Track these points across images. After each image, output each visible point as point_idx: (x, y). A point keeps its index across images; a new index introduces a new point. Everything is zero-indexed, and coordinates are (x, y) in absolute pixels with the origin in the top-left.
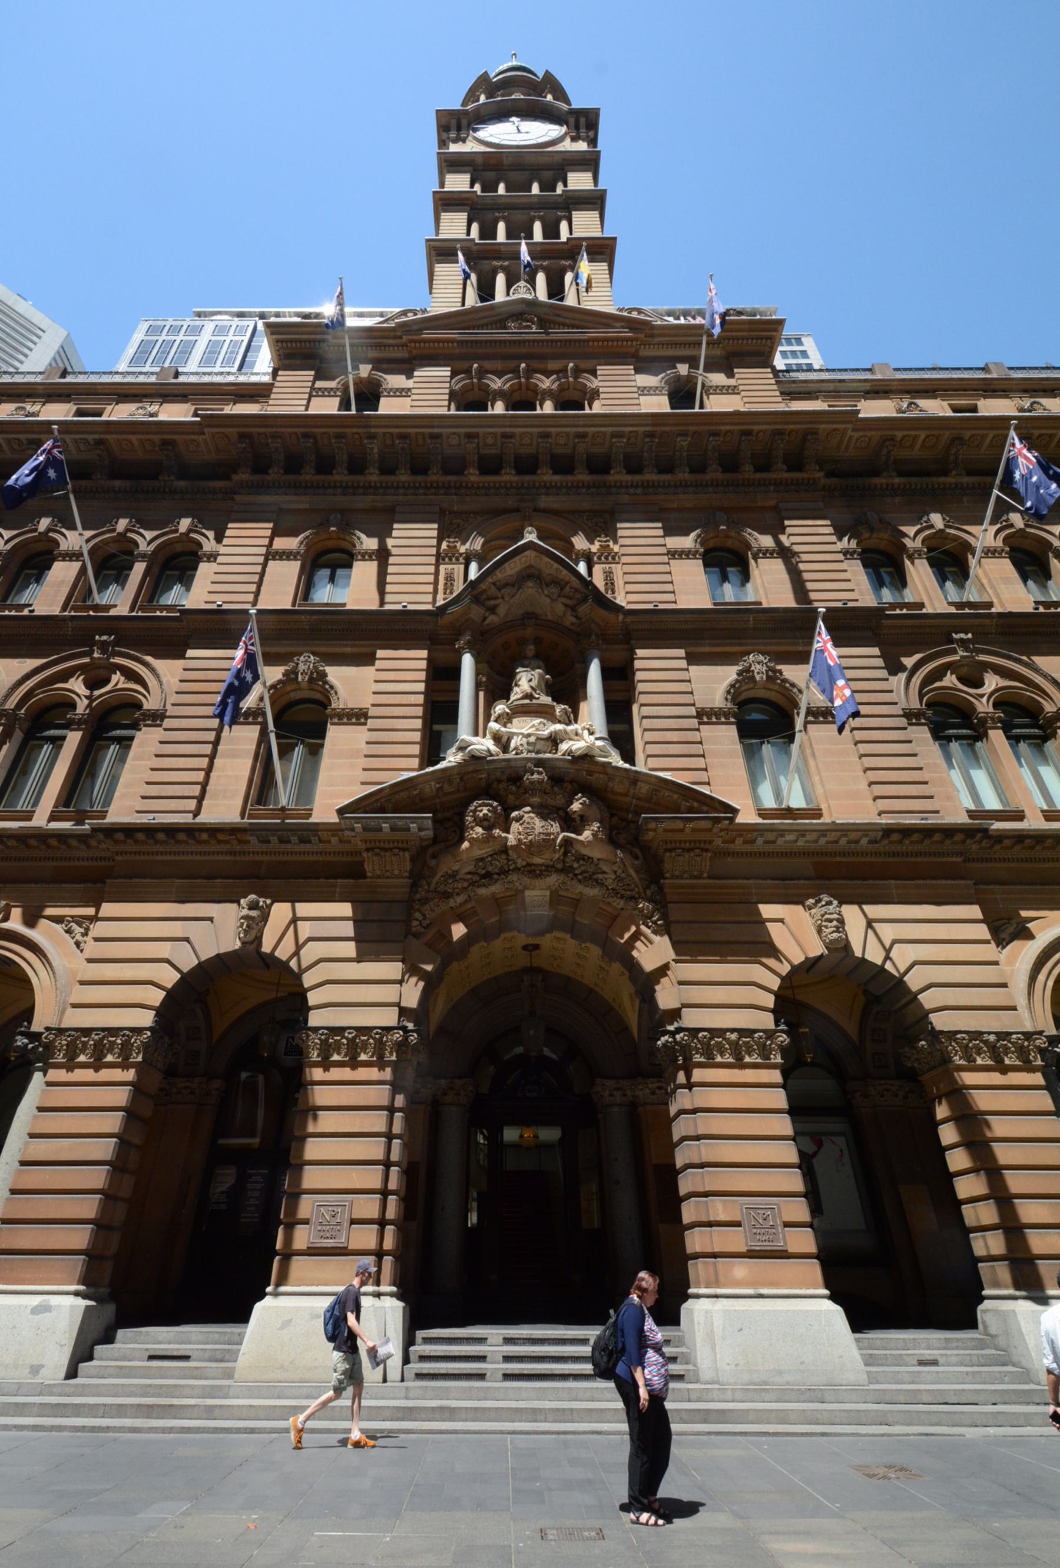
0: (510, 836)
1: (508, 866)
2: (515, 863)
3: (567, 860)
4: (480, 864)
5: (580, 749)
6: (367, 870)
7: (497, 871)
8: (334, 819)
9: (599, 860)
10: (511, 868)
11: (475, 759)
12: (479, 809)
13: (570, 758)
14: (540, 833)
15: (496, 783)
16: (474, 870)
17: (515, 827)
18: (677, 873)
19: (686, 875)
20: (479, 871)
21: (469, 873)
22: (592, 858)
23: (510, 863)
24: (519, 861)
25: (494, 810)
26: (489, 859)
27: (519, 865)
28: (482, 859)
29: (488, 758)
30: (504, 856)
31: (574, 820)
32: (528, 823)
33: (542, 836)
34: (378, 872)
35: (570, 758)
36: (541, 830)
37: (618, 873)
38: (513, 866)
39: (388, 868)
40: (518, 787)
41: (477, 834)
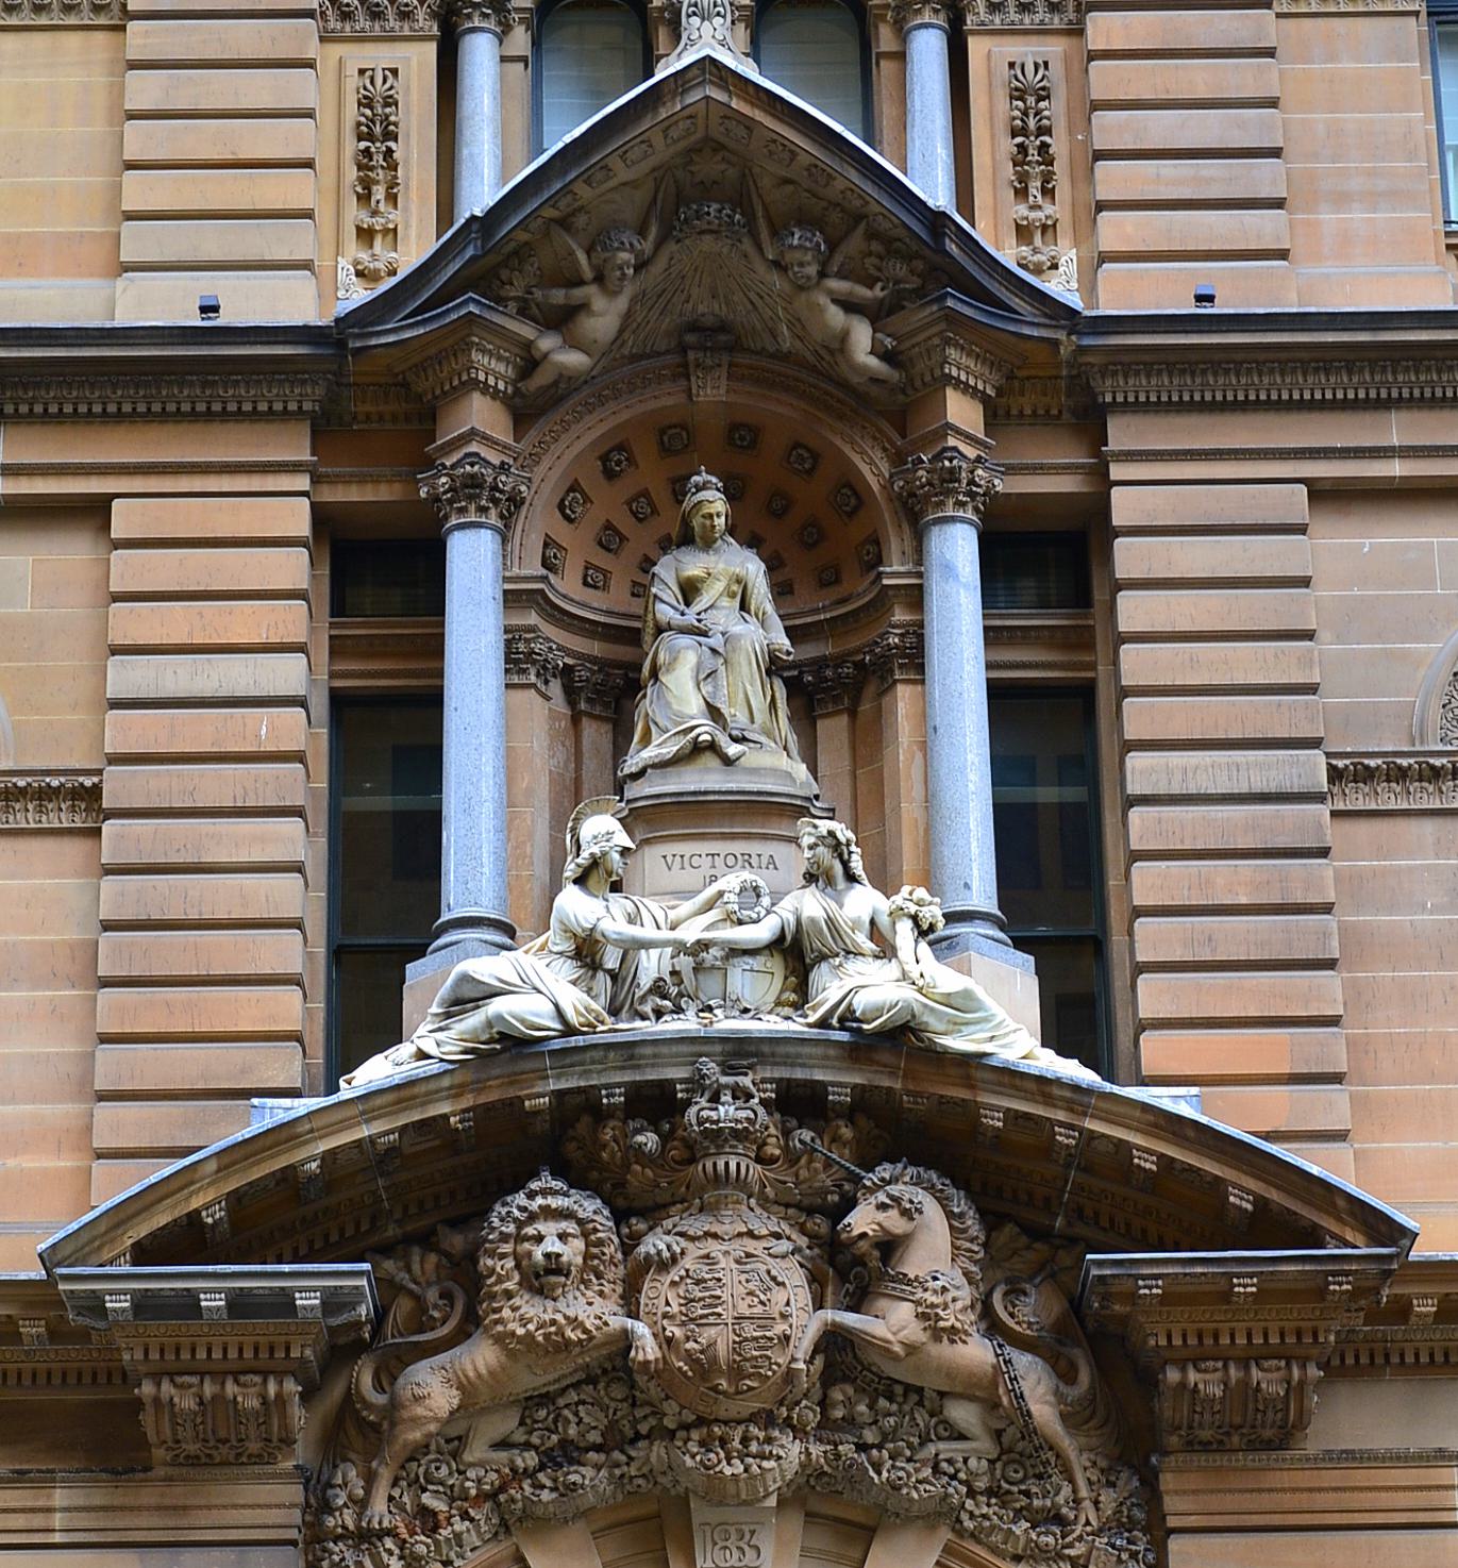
0: (641, 1329)
1: (635, 1422)
2: (659, 1414)
3: (837, 1395)
4: (543, 1413)
5: (879, 1011)
6: (152, 1437)
7: (594, 1437)
8: (37, 1273)
9: (942, 1395)
10: (644, 1428)
11: (510, 1044)
12: (530, 1231)
13: (843, 1036)
14: (740, 1318)
15: (586, 1120)
16: (520, 1437)
17: (660, 1293)
18: (1205, 1434)
19: (1236, 1439)
20: (535, 1440)
21: (503, 1444)
22: (920, 1390)
23: (639, 1413)
24: (671, 1407)
25: (586, 1229)
26: (573, 1396)
27: (669, 1423)
28: (545, 1399)
29: (557, 1044)
30: (618, 1391)
31: (860, 1261)
32: (698, 1282)
33: (750, 1330)
34: (192, 1448)
35: (843, 1036)
36: (743, 1309)
37: (1005, 1439)
38: (653, 1421)
39: (222, 1434)
40: (665, 1139)
41: (524, 1321)
